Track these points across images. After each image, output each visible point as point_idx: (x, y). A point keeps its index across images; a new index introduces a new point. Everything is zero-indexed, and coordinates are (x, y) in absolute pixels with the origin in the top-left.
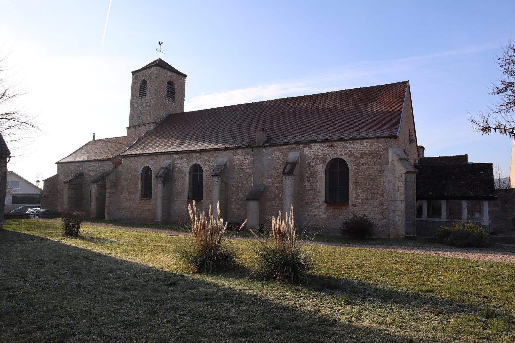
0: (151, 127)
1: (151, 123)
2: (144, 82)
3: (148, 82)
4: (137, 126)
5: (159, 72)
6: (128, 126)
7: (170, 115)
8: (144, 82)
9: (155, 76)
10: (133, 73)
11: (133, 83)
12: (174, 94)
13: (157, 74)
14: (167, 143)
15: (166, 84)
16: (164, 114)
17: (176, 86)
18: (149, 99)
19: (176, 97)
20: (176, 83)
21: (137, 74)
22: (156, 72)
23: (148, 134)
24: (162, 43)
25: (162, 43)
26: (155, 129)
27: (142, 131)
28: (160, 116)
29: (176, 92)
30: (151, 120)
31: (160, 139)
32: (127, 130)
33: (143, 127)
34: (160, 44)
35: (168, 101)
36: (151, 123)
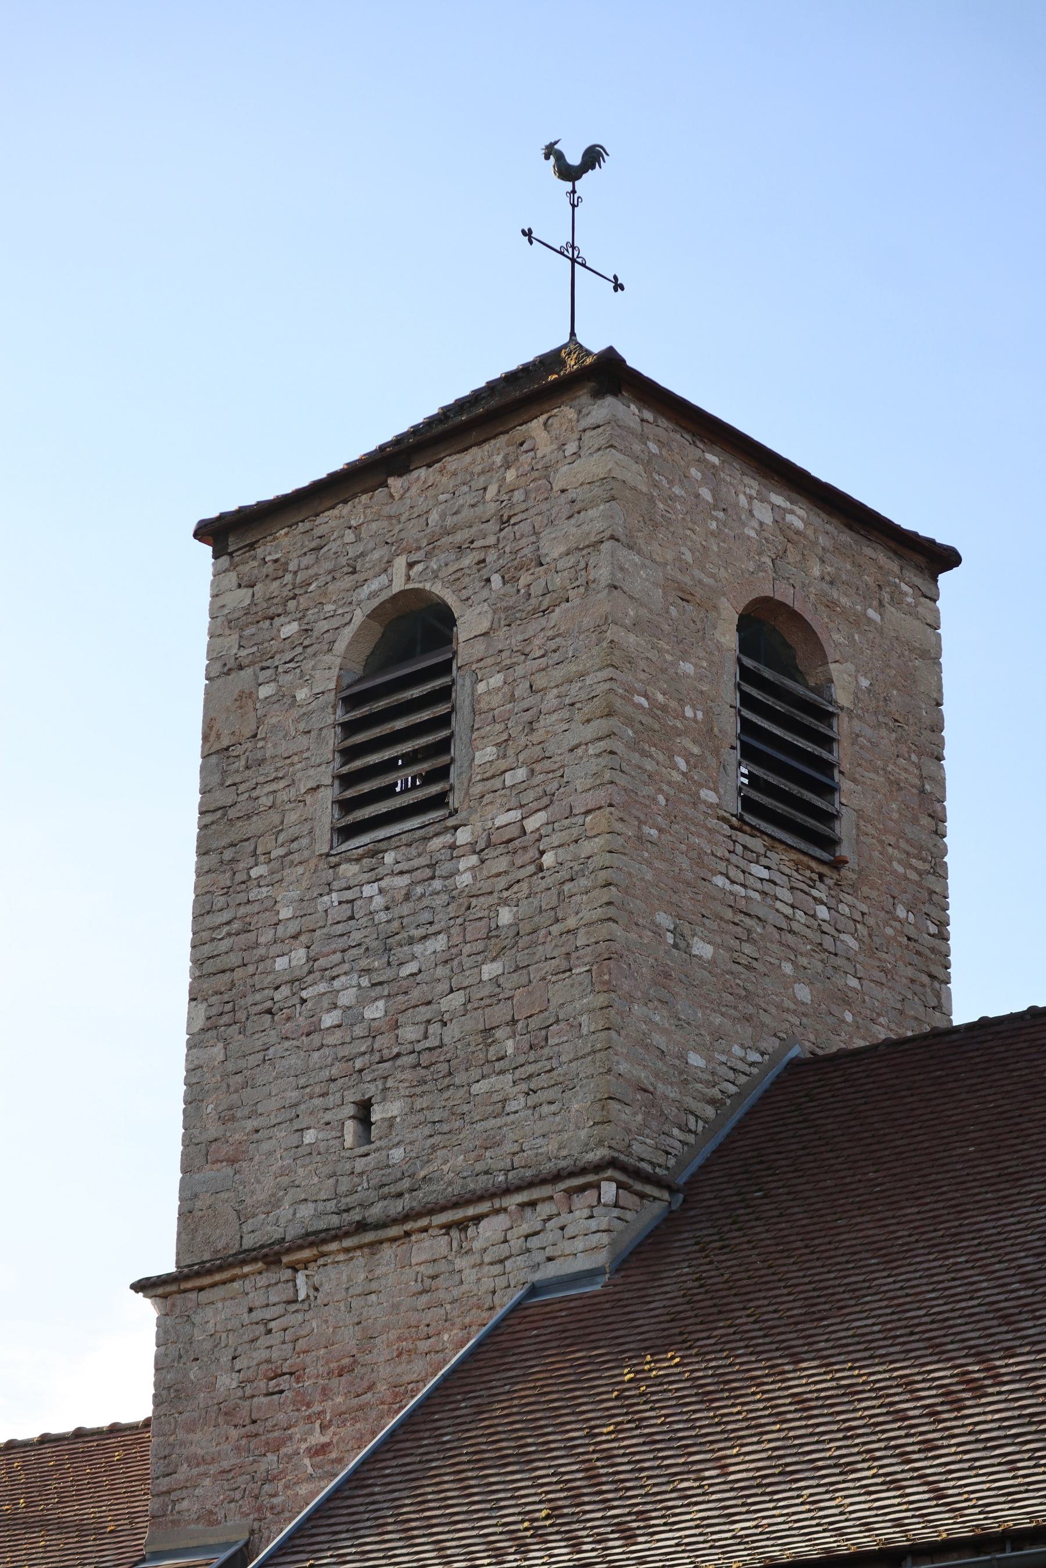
0: (582, 1239)
1: (575, 1177)
2: (415, 633)
3: (470, 623)
4: (316, 1239)
5: (634, 474)
6: (167, 1265)
7: (796, 1065)
8: (415, 633)
9: (596, 520)
10: (216, 532)
11: (222, 669)
12: (828, 790)
13: (612, 491)
14: (984, 1414)
15: (730, 639)
16: (722, 1058)
17: (845, 682)
18: (512, 841)
19: (843, 829)
20: (834, 637)
21: (284, 542)
22: (593, 466)
23: (535, 1340)
24: (593, 157)
25: (593, 157)
26: (640, 1258)
27: (412, 1313)
28: (685, 1078)
29: (842, 755)
30: (566, 1131)
31: (808, 1379)
32: (146, 1312)
33: (429, 1247)
34: (568, 173)
35: (766, 874)
36: (575, 1177)
